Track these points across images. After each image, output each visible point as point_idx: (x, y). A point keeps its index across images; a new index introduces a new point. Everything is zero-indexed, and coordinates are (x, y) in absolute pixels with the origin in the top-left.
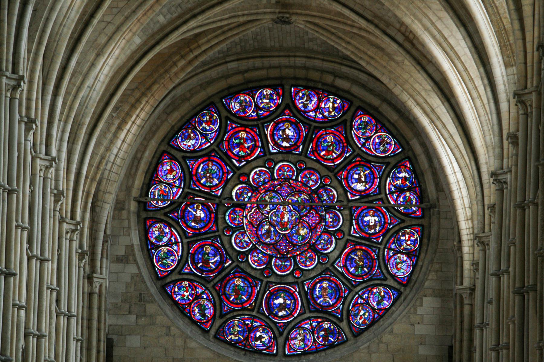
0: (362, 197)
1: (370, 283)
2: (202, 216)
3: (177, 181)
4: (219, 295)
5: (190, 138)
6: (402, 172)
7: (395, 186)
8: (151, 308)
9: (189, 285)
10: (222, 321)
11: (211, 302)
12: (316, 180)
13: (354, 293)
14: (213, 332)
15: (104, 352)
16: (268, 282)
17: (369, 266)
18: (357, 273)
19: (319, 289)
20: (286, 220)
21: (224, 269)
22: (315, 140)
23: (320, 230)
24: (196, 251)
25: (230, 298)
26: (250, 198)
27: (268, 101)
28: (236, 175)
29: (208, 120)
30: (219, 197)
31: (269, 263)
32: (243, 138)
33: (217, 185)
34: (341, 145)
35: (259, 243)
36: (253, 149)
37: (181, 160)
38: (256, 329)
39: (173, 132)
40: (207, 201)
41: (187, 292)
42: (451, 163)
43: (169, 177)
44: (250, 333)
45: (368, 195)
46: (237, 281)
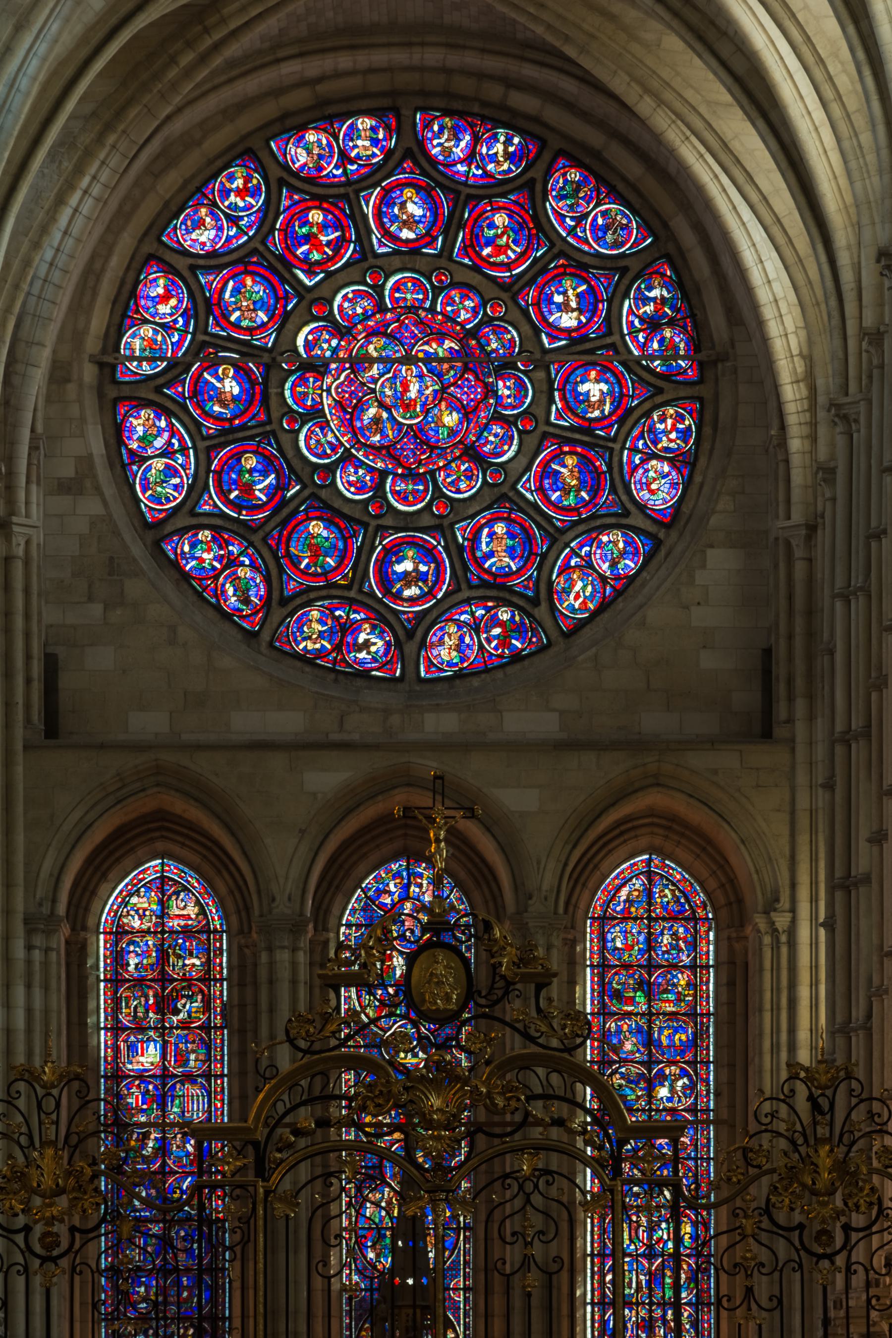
0: (573, 342)
2: (236, 390)
3: (180, 319)
4: (277, 559)
8: (134, 588)
9: (213, 537)
11: (261, 572)
12: (474, 308)
14: (266, 636)
15: (39, 681)
16: (379, 528)
17: (592, 486)
18: (566, 503)
20: (413, 393)
21: (284, 502)
22: (470, 224)
24: (223, 463)
25: (301, 563)
26: (335, 351)
27: (367, 143)
28: (304, 303)
30: (270, 351)
31: (379, 487)
33: (263, 326)
34: (526, 232)
35: (360, 445)
37: (186, 273)
40: (246, 359)
42: (761, 262)
44: (344, 636)
45: (585, 339)
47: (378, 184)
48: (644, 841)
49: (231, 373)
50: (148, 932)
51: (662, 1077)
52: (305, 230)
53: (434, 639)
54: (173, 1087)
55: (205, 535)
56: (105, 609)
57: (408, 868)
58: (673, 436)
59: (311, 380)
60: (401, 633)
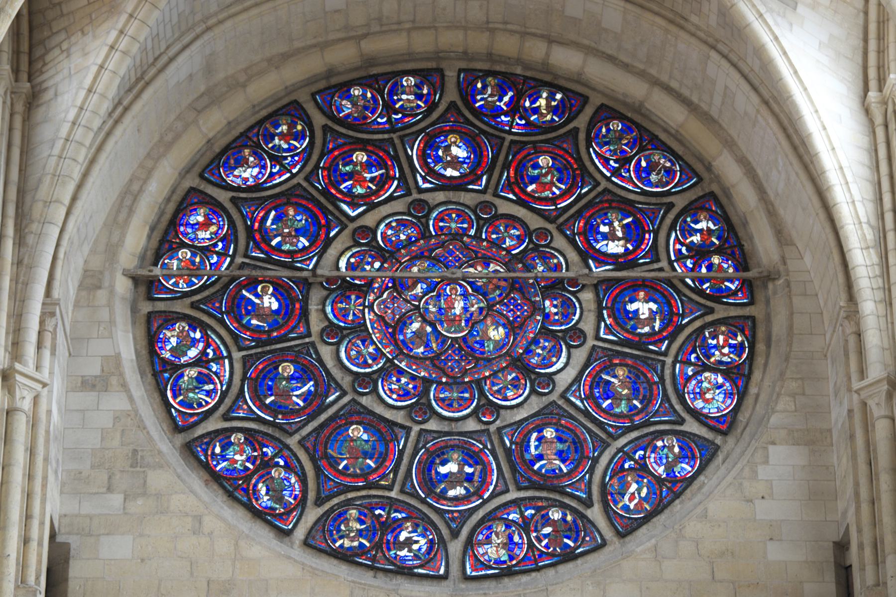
2: (275, 306)
4: (313, 460)
5: (247, 164)
6: (702, 221)
9: (245, 438)
10: (321, 511)
11: (296, 474)
14: (300, 533)
17: (644, 396)
18: (618, 410)
19: (537, 443)
25: (339, 464)
27: (412, 97)
28: (347, 232)
29: (285, 131)
32: (361, 163)
36: (382, 182)
38: (398, 526)
39: (209, 156)
41: (242, 455)
43: (203, 236)
46: (353, 430)
49: (271, 290)
56: (125, 499)
58: (726, 350)
59: (353, 297)
60: (445, 532)
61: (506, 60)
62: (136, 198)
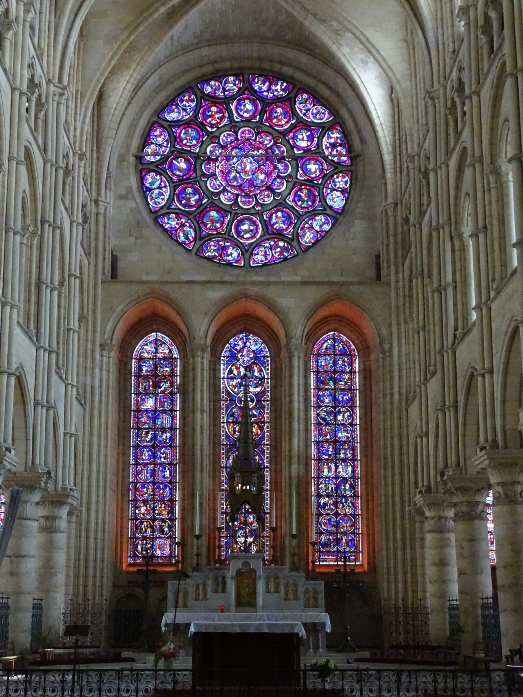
1: (313, 213)
4: (199, 224)
7: (330, 144)
8: (146, 232)
13: (301, 220)
14: (194, 251)
16: (236, 213)
20: (248, 168)
21: (201, 205)
23: (274, 175)
24: (179, 191)
26: (220, 154)
28: (210, 138)
30: (197, 153)
31: (236, 199)
33: (195, 145)
35: (228, 185)
36: (222, 119)
39: (161, 108)
47: (236, 98)
48: (332, 326)
50: (150, 358)
51: (339, 412)
52: (210, 113)
53: (256, 252)
54: (158, 415)
55: (173, 216)
57: (246, 336)
58: (342, 183)
60: (243, 250)
61: (266, 70)
62: (136, 127)
